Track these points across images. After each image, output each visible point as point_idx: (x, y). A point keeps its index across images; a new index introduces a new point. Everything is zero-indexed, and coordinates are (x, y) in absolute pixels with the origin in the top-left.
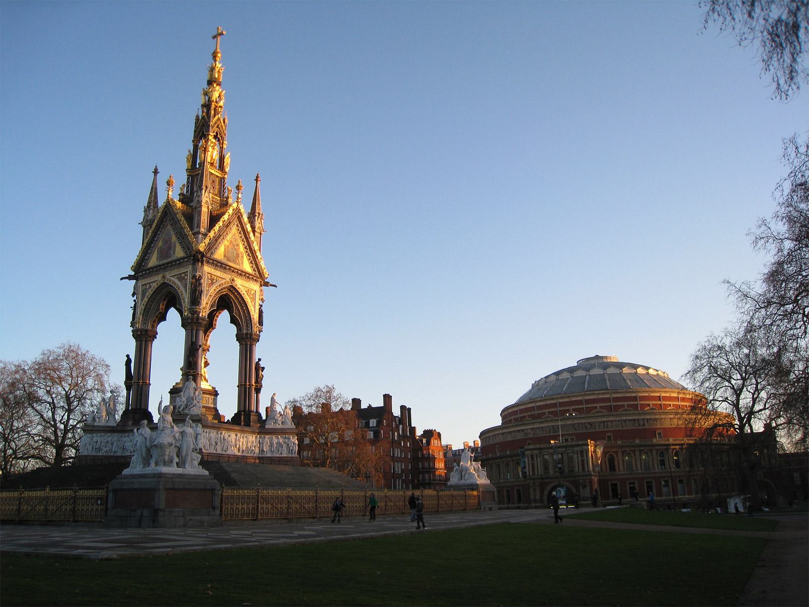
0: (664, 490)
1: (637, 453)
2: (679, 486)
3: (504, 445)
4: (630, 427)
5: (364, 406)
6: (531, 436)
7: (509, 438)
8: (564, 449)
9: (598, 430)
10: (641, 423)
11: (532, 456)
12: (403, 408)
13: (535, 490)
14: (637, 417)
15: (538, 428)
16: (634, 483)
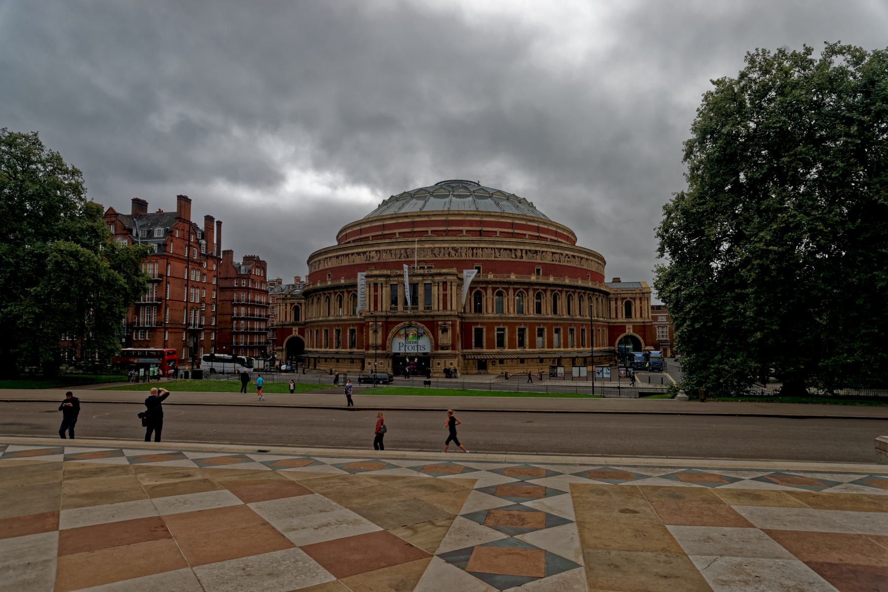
0: (539, 340)
1: (511, 292)
2: (556, 336)
3: (336, 272)
4: (504, 257)
5: (151, 210)
6: (375, 260)
7: (345, 262)
8: (420, 278)
9: (463, 258)
10: (519, 254)
11: (376, 285)
12: (209, 219)
13: (375, 331)
14: (514, 247)
15: (386, 251)
16: (503, 330)
